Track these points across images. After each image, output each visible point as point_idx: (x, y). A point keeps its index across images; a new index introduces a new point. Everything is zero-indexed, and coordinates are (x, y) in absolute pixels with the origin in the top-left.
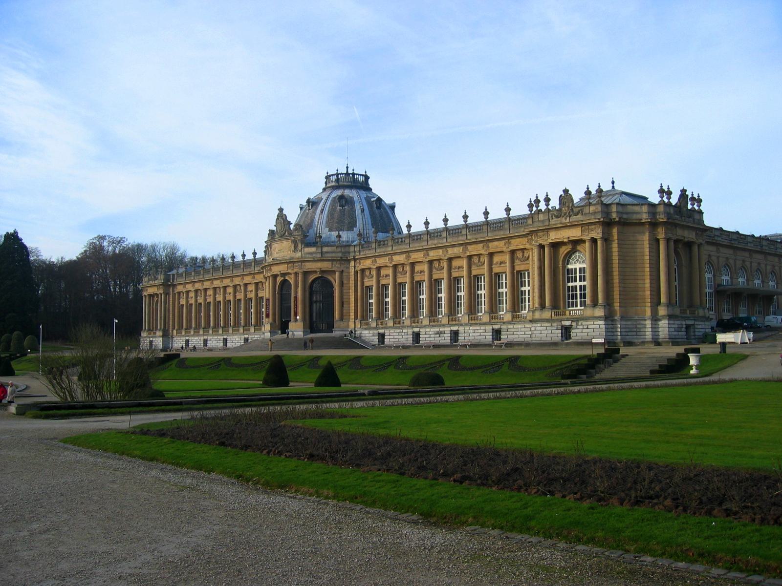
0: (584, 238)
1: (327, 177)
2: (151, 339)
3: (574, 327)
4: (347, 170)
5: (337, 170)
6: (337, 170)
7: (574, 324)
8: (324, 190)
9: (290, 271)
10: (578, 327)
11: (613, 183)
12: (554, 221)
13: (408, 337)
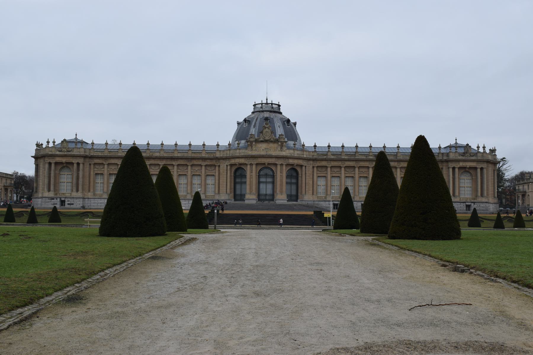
0: (478, 167)
1: (255, 105)
2: (63, 199)
3: (472, 205)
4: (267, 102)
5: (262, 101)
6: (262, 101)
7: (472, 204)
8: (253, 113)
9: (277, 163)
10: (475, 205)
11: (456, 140)
12: (461, 158)
13: (357, 206)
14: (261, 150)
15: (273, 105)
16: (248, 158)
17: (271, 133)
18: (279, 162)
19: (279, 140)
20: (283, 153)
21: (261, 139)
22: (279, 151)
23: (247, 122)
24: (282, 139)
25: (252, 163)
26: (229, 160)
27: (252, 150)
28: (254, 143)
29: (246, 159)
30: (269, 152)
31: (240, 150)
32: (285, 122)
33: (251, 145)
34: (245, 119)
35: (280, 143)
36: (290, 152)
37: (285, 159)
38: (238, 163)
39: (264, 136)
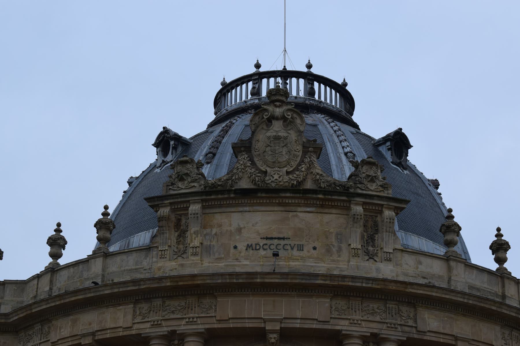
9: (343, 326)
14: (241, 246)
15: (316, 84)
16: (158, 302)
17: (305, 152)
18: (353, 323)
19: (352, 190)
20: (378, 270)
21: (245, 184)
22: (356, 255)
23: (175, 148)
24: (373, 187)
25: (182, 327)
26: (46, 328)
27: (181, 253)
28: (195, 208)
29: (145, 306)
30: (290, 258)
31: (109, 261)
32: (383, 149)
33: (179, 220)
34: (161, 133)
35: (359, 209)
36: (422, 268)
37: (391, 305)
38: (93, 334)
39: (259, 164)
